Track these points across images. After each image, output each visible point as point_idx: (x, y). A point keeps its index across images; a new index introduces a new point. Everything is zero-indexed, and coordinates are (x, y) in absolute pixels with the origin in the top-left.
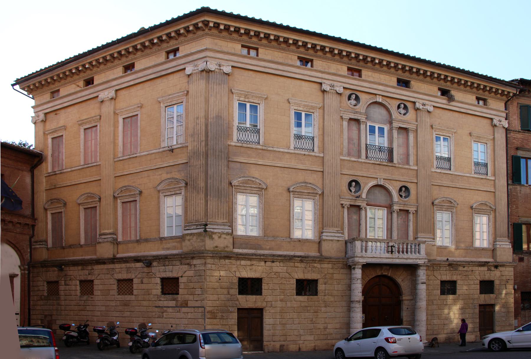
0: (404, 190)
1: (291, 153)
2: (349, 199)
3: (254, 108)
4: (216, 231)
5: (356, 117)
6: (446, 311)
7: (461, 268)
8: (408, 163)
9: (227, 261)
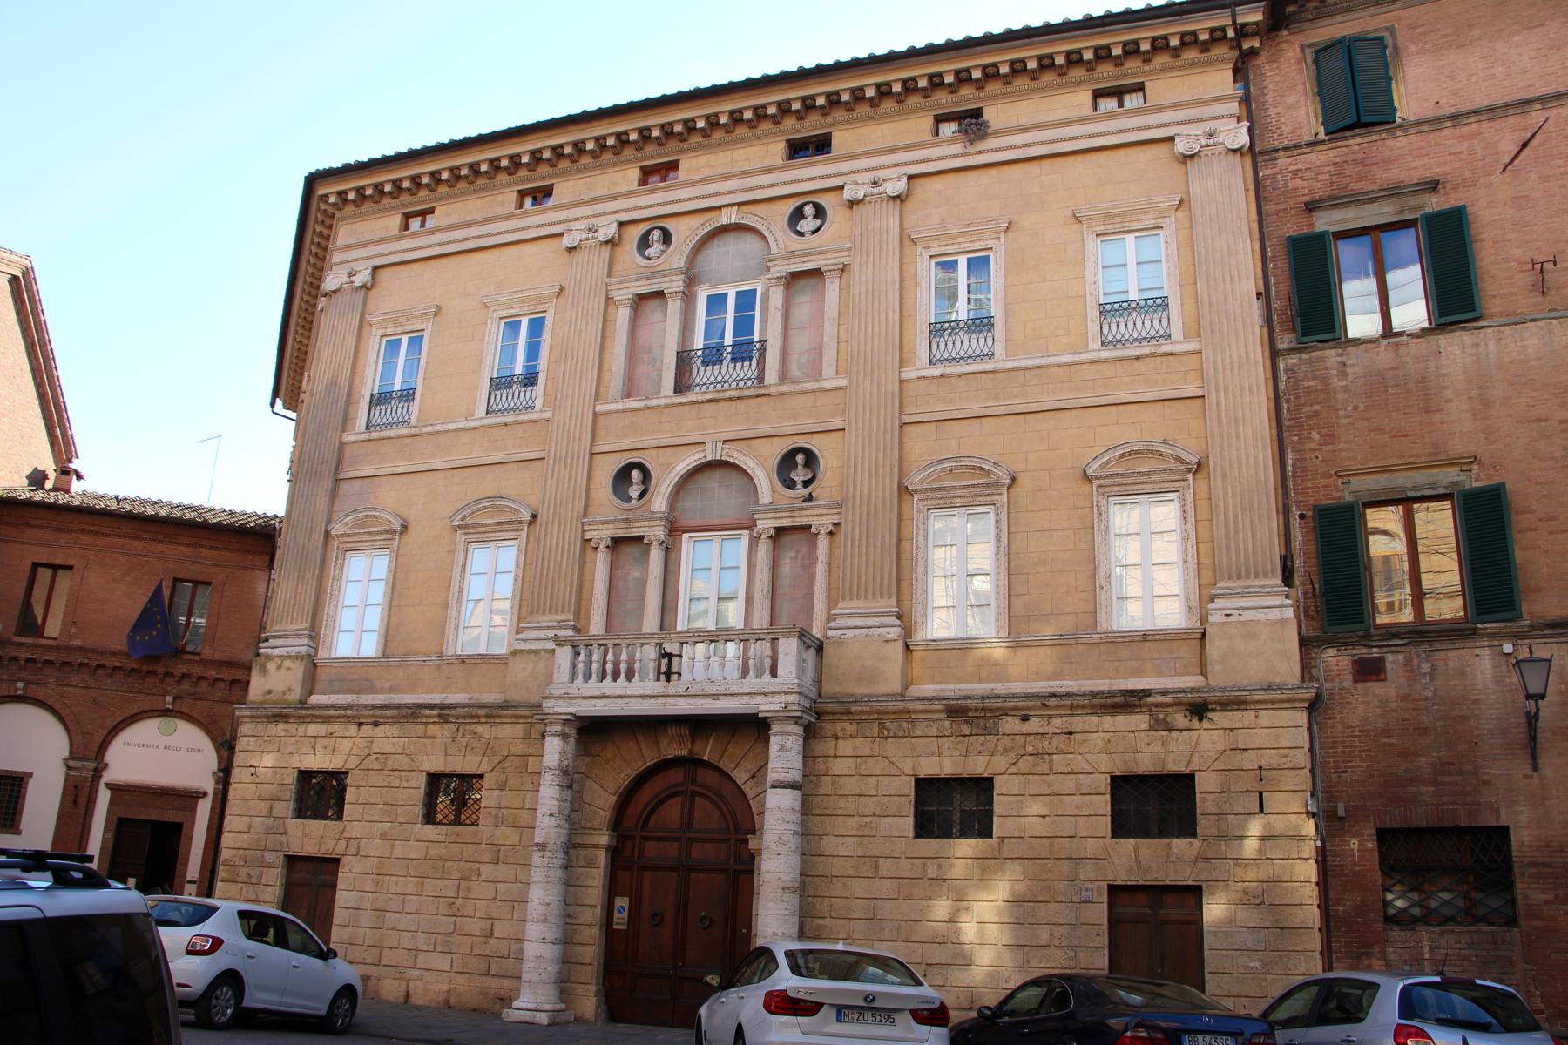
0: (797, 463)
1: (475, 428)
2: (607, 522)
3: (416, 343)
4: (276, 652)
5: (655, 288)
6: (941, 910)
7: (1010, 725)
8: (819, 376)
9: (281, 726)
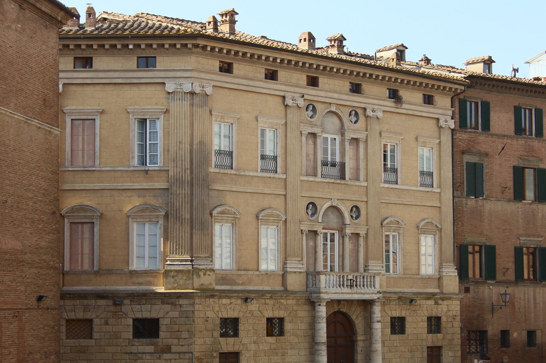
4: (201, 267)
9: (211, 300)
